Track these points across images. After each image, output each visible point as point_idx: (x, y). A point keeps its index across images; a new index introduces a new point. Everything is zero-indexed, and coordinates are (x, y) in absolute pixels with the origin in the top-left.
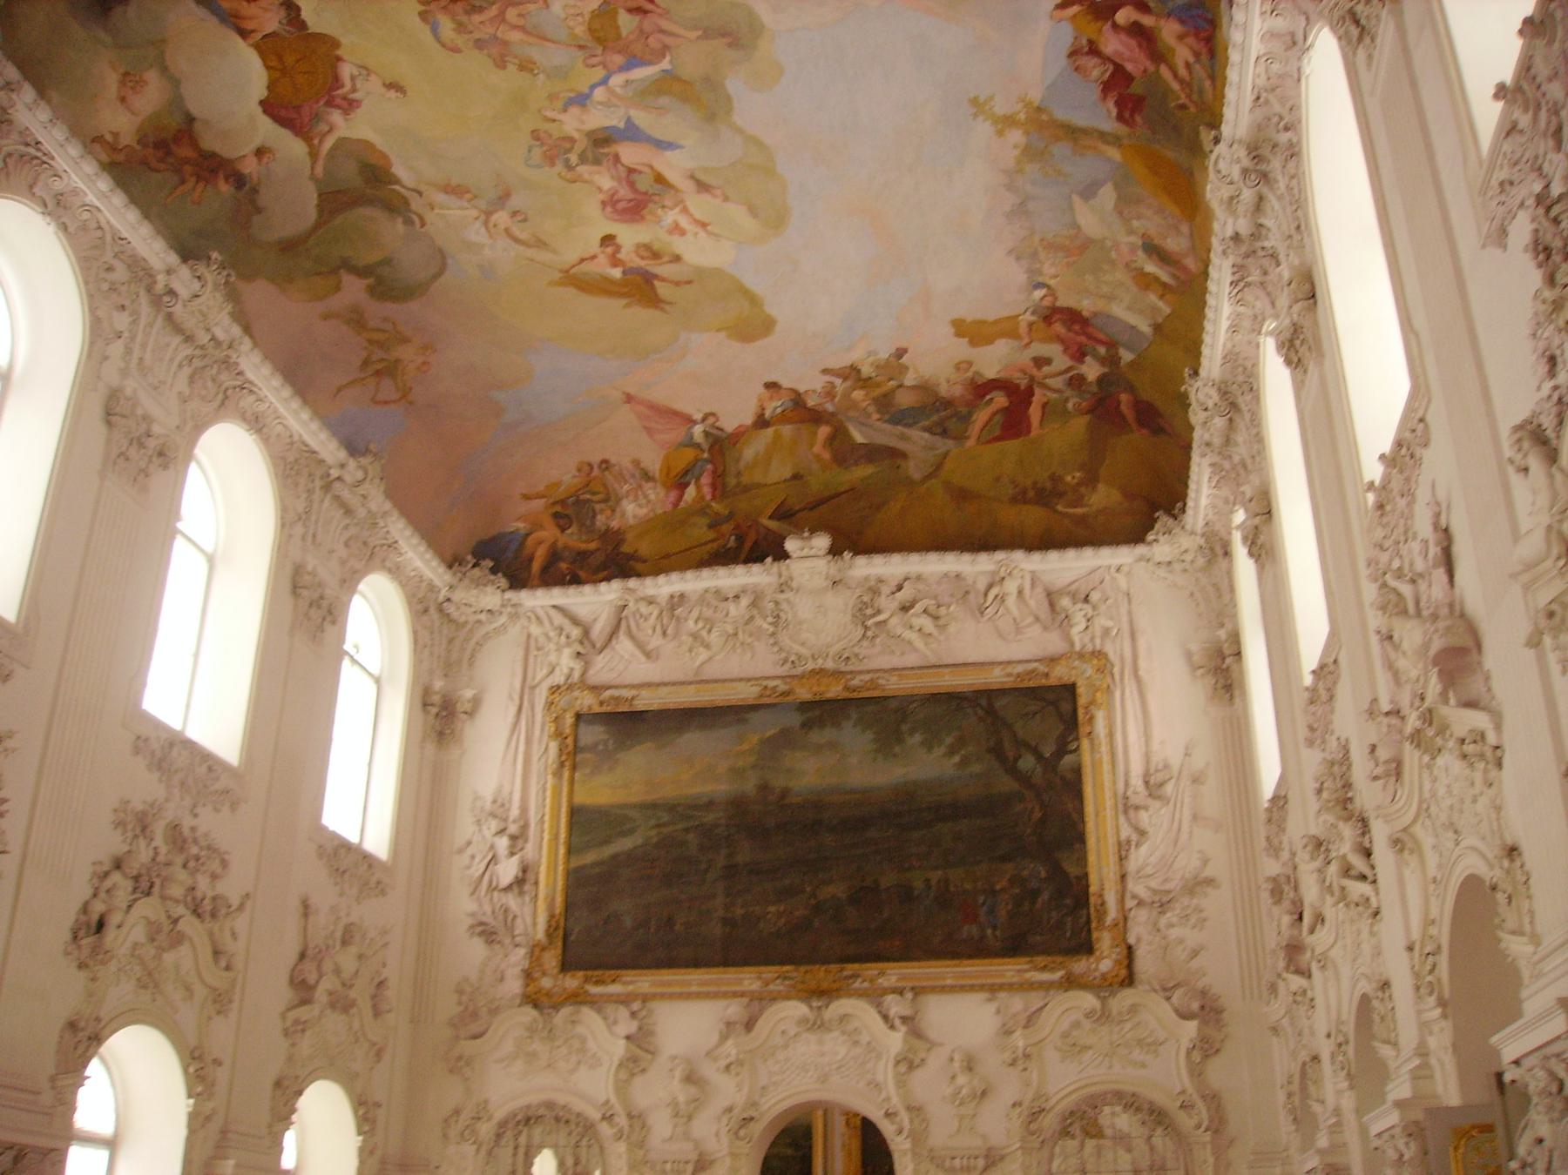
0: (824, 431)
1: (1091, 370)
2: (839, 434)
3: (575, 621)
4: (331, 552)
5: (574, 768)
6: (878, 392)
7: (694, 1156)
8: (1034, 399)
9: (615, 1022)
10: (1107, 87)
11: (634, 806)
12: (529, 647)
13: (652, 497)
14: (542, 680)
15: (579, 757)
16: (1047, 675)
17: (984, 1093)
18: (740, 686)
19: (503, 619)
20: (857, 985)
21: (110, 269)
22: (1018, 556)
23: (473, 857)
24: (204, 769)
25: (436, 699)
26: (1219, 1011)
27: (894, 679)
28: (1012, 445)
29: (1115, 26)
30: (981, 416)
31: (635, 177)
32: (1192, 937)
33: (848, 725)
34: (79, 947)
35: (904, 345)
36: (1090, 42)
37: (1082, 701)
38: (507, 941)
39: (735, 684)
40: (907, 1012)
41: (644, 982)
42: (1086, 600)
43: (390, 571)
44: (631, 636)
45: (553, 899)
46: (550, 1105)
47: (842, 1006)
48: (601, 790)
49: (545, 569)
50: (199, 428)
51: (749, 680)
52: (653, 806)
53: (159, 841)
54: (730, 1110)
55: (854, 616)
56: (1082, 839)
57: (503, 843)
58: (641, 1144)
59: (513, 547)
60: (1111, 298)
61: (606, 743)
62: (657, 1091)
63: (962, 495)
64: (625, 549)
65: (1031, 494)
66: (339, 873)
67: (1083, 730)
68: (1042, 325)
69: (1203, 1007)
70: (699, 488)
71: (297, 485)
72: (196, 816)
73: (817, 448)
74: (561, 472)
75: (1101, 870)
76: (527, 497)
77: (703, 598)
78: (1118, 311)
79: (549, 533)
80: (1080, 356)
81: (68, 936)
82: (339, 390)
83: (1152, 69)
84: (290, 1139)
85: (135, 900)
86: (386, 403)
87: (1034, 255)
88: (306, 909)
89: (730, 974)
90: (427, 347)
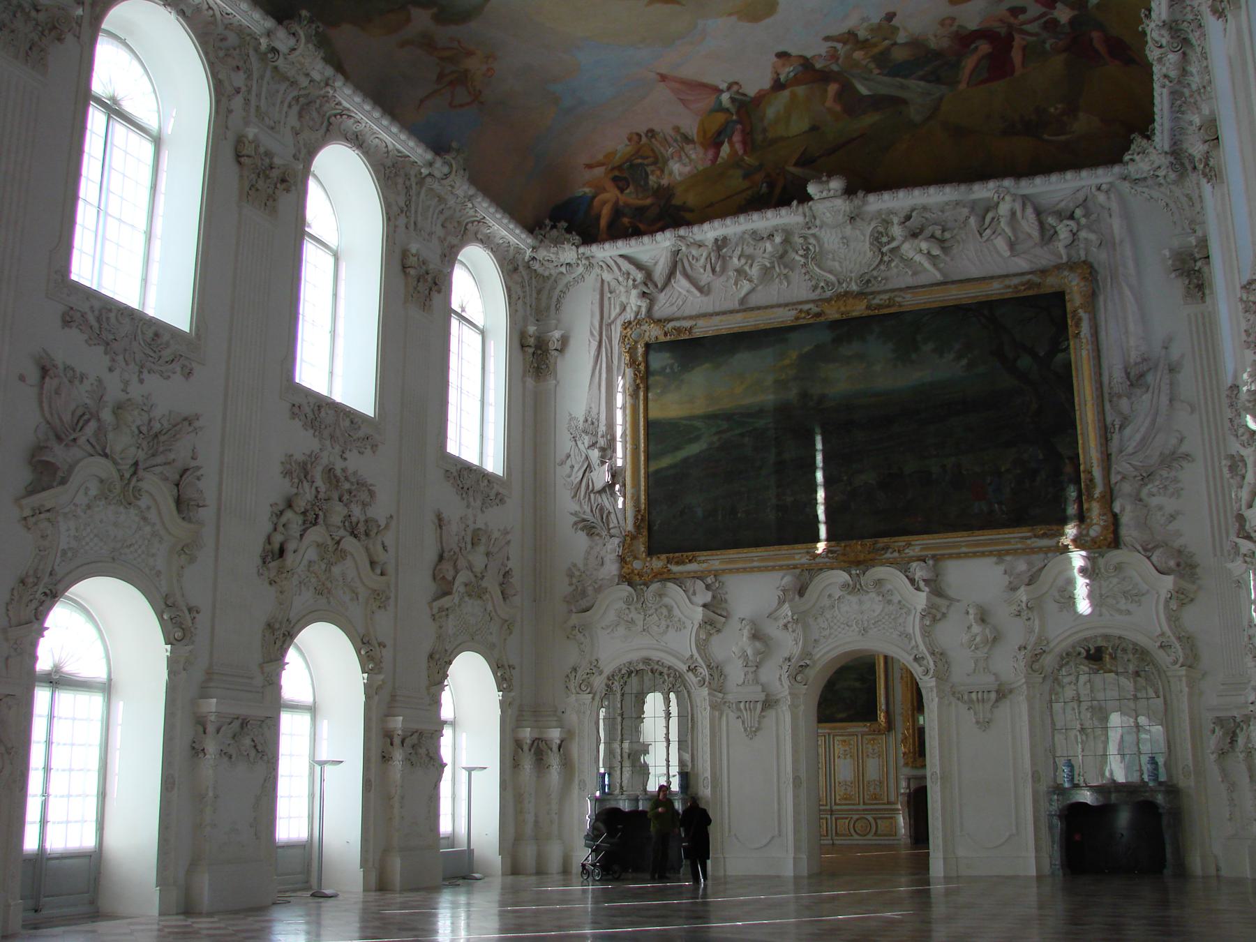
0: (833, 88)
1: (1063, 14)
2: (846, 90)
3: (639, 266)
4: (431, 234)
5: (647, 390)
6: (876, 50)
7: (762, 697)
8: (1016, 44)
12: (603, 290)
13: (693, 156)
14: (616, 319)
15: (652, 380)
17: (995, 639)
18: (780, 311)
19: (581, 269)
20: (888, 555)
21: (224, 39)
22: (1008, 183)
23: (572, 467)
24: (347, 423)
25: (532, 341)
26: (1193, 567)
27: (908, 296)
30: (969, 63)
34: (268, 569)
35: (891, 9)
38: (604, 533)
39: (775, 310)
41: (714, 561)
42: (1071, 217)
43: (482, 241)
45: (639, 497)
46: (647, 661)
49: (611, 225)
50: (312, 153)
51: (786, 305)
53: (319, 483)
55: (871, 244)
56: (1073, 426)
57: (595, 454)
58: (721, 689)
62: (732, 646)
64: (676, 201)
66: (464, 490)
69: (1178, 565)
70: (732, 145)
71: (396, 184)
72: (345, 459)
73: (829, 103)
74: (614, 142)
76: (590, 166)
77: (742, 238)
81: (260, 561)
82: (422, 101)
84: (446, 697)
85: (305, 530)
86: (461, 106)
88: (440, 522)
89: (784, 550)
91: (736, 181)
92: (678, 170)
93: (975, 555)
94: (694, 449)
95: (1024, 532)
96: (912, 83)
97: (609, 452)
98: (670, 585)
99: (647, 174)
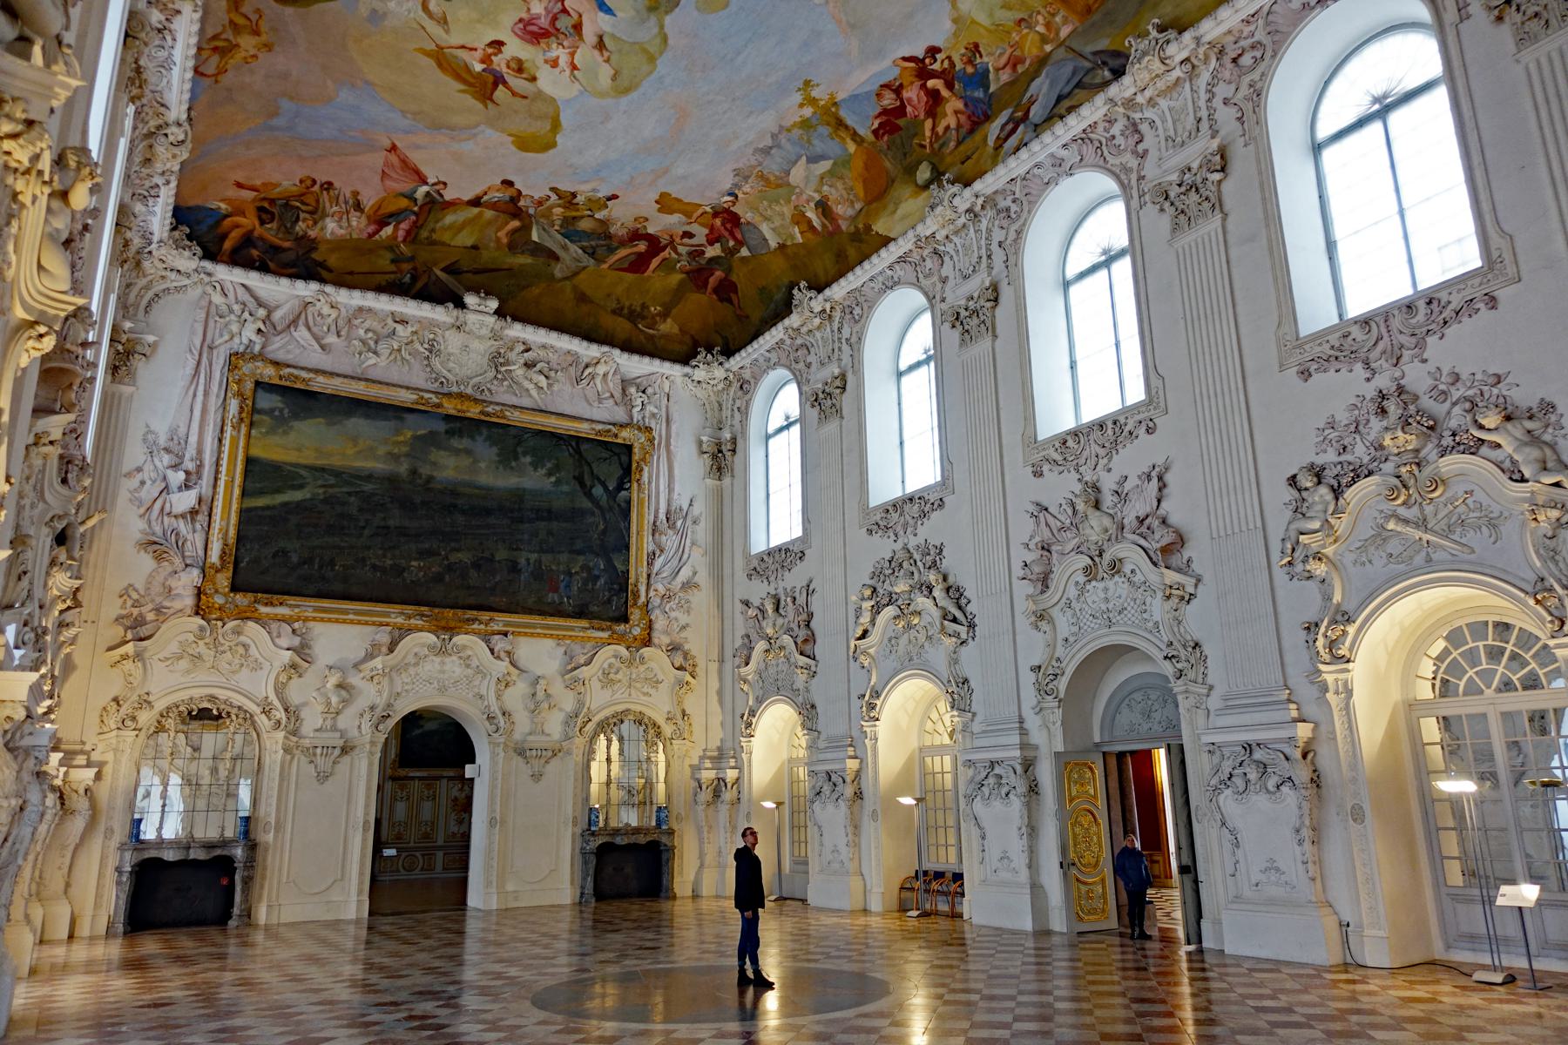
0: (515, 224)
1: (713, 251)
2: (526, 228)
5: (252, 424)
6: (574, 214)
7: (341, 743)
9: (279, 636)
10: (885, 112)
11: (306, 467)
12: (210, 312)
13: (354, 223)
16: (616, 436)
19: (187, 282)
22: (616, 352)
23: (143, 483)
27: (517, 414)
28: (630, 277)
29: (923, 86)
30: (622, 252)
31: (563, 17)
32: (683, 619)
33: (480, 439)
36: (901, 86)
37: (636, 457)
38: (178, 561)
40: (509, 648)
41: (309, 606)
44: (309, 329)
47: (460, 639)
48: (275, 449)
51: (408, 388)
52: (323, 469)
54: (372, 708)
56: (627, 548)
58: (295, 733)
59: (210, 221)
60: (767, 219)
61: (281, 411)
63: (582, 298)
64: (315, 256)
67: (635, 476)
70: (396, 228)
73: (502, 234)
74: (285, 178)
75: (637, 571)
76: (239, 185)
78: (765, 229)
79: (249, 221)
80: (711, 243)
83: (922, 116)
87: (746, 178)
89: (380, 608)
90: (268, 47)
91: (384, 262)
92: (331, 227)
93: (545, 635)
94: (297, 496)
95: (584, 623)
96: (575, 249)
97: (194, 477)
98: (251, 623)
99: (298, 219)
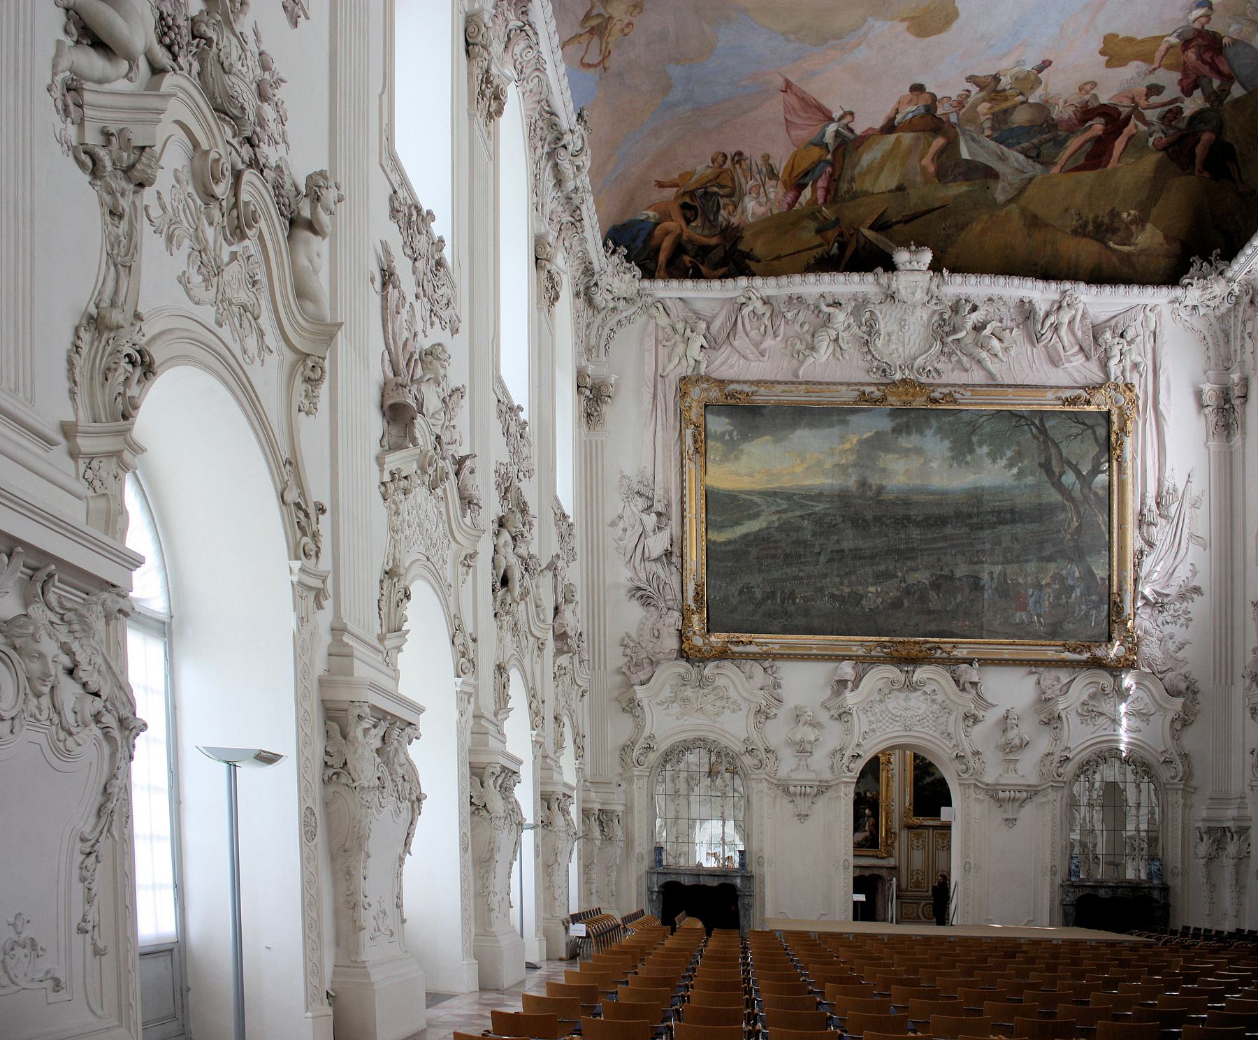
1: (1193, 104)
63: (1034, 222)
65: (1090, 227)
68: (1179, 50)
73: (926, 161)
80: (1188, 92)
96: (1015, 157)
